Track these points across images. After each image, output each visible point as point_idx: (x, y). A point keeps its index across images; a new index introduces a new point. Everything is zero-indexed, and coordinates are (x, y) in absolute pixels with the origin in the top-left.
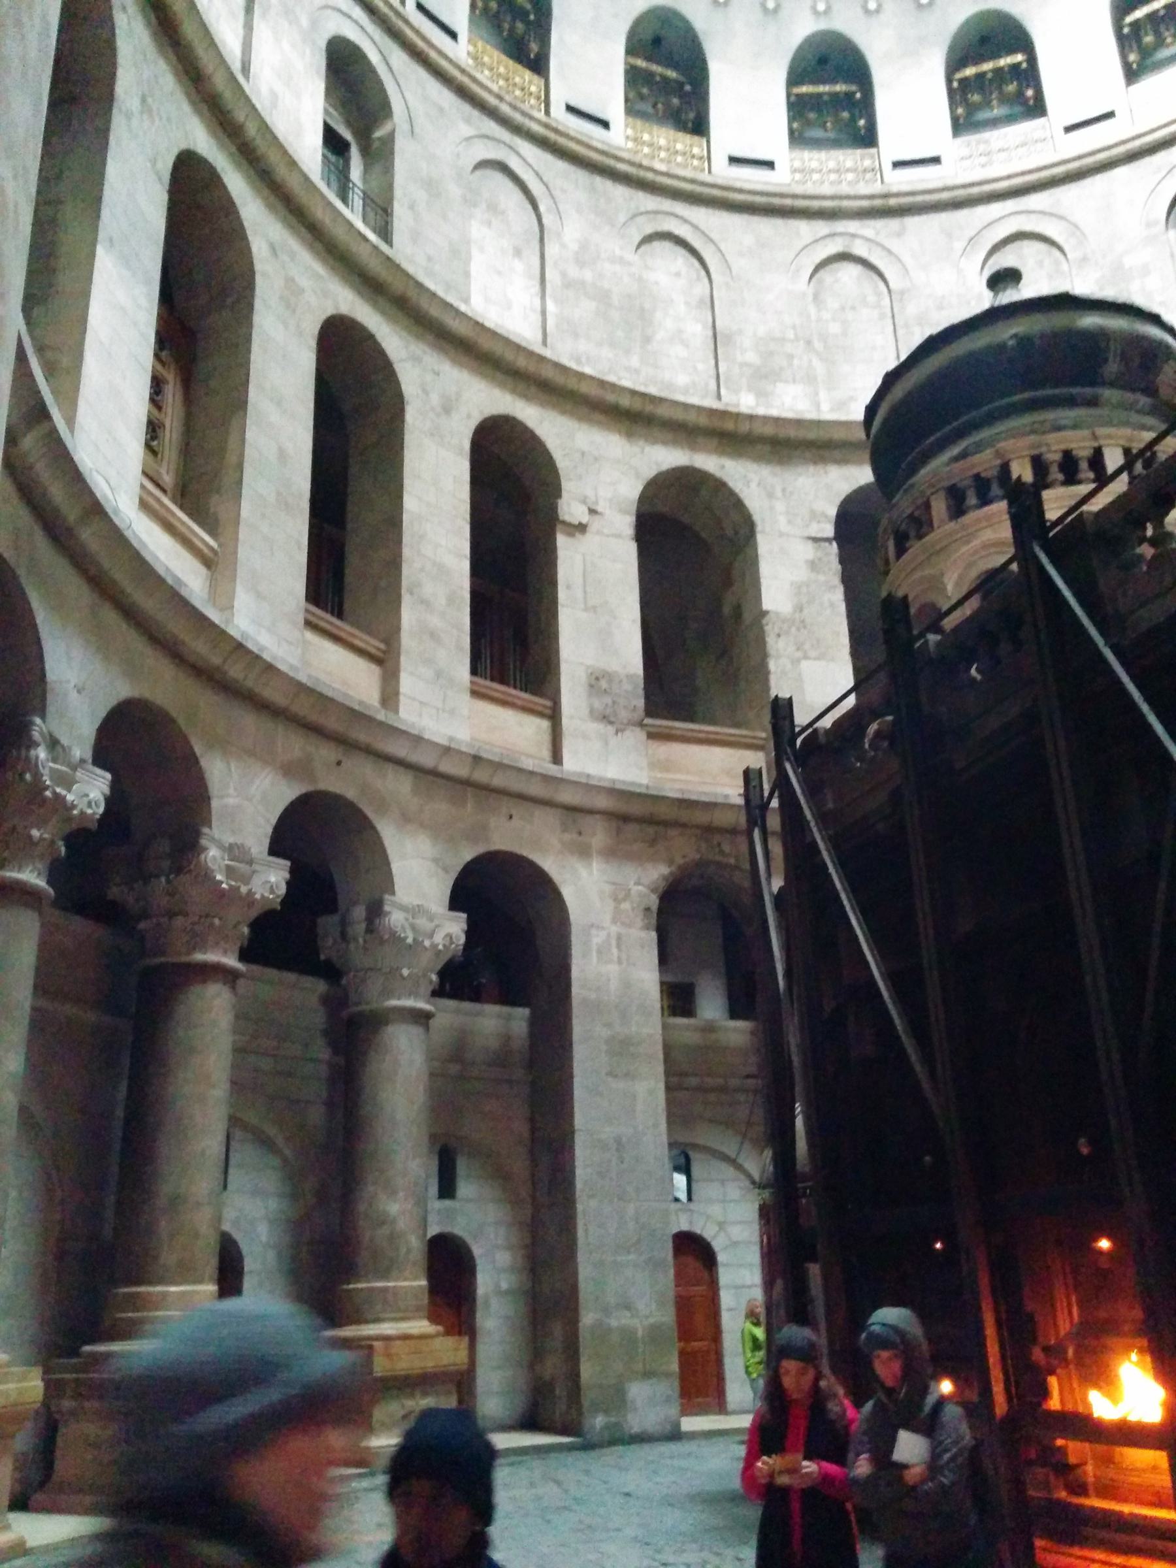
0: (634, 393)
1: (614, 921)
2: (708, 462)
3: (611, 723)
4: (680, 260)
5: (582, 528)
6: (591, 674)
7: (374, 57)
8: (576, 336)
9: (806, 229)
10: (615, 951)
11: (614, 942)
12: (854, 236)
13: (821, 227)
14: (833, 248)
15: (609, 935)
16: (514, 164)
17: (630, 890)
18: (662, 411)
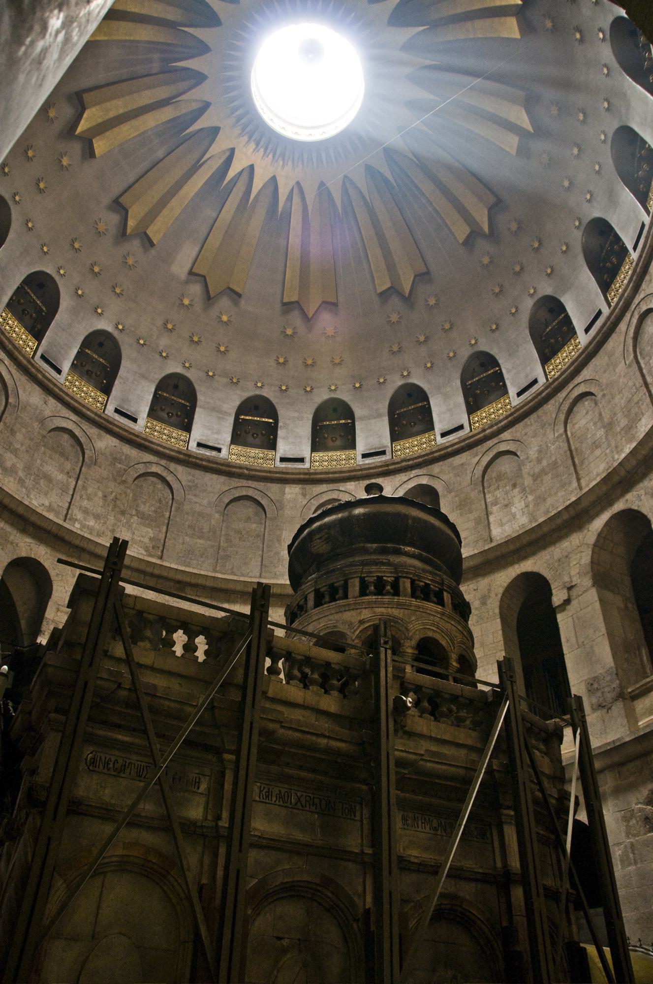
0: (567, 508)
1: (628, 837)
2: (619, 506)
3: (604, 707)
4: (587, 403)
5: (567, 602)
6: (588, 684)
7: (424, 481)
8: (544, 500)
9: (622, 326)
10: (631, 856)
11: (630, 850)
12: (639, 304)
13: (628, 315)
14: (635, 321)
15: (625, 846)
16: (503, 447)
17: (633, 810)
18: (585, 503)
